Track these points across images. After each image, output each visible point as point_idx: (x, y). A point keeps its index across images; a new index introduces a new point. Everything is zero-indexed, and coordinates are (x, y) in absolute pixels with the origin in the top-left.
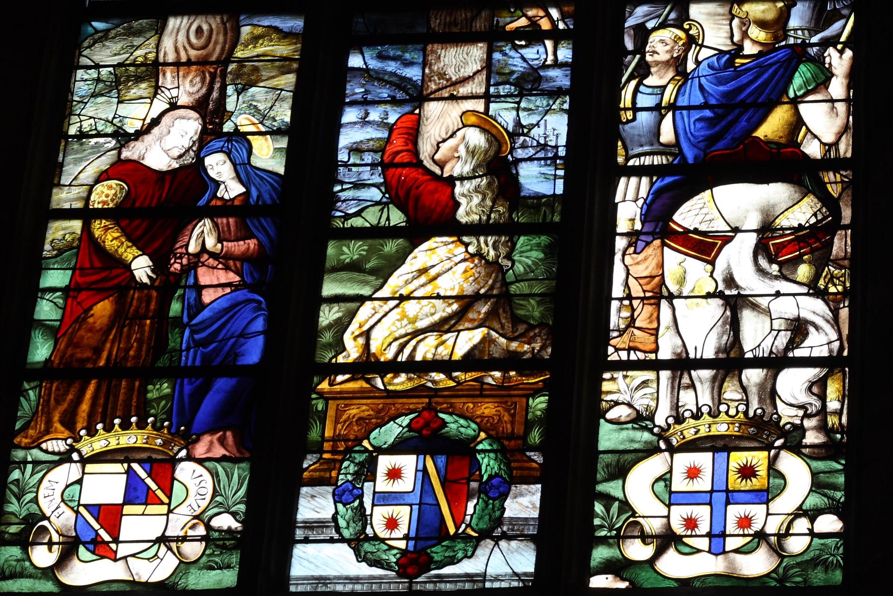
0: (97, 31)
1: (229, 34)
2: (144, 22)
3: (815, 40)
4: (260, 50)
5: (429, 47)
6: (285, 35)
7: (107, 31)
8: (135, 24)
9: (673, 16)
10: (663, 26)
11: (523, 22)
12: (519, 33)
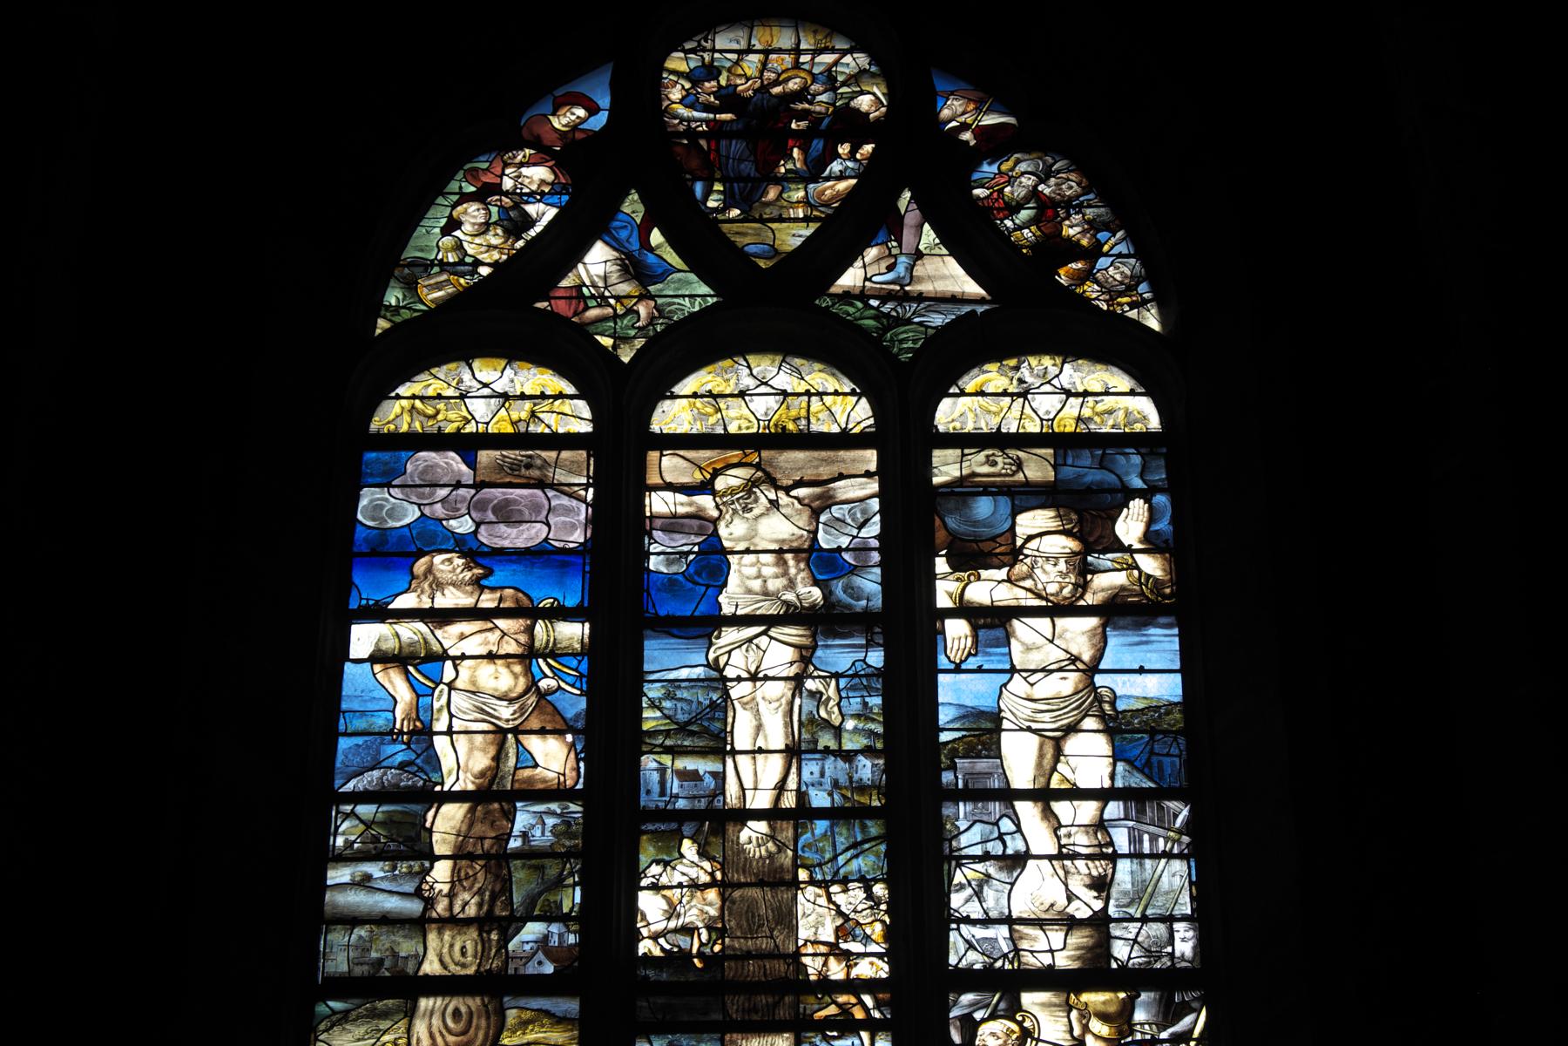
0: (334, 1012)
1: (493, 1018)
2: (390, 1002)
3: (1164, 1035)
4: (530, 1037)
5: (727, 1037)
6: (559, 1020)
7: (347, 1012)
8: (380, 1005)
9: (1002, 1005)
10: (993, 1017)
11: (832, 1010)
12: (828, 1023)
